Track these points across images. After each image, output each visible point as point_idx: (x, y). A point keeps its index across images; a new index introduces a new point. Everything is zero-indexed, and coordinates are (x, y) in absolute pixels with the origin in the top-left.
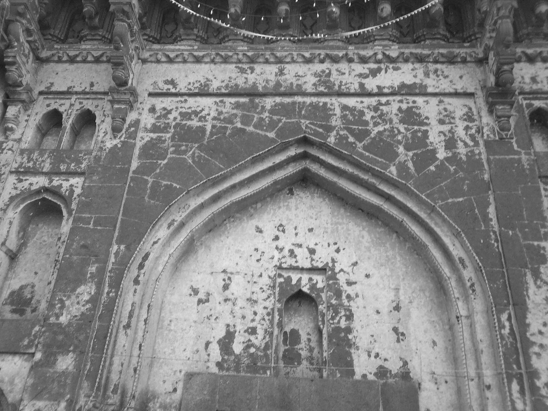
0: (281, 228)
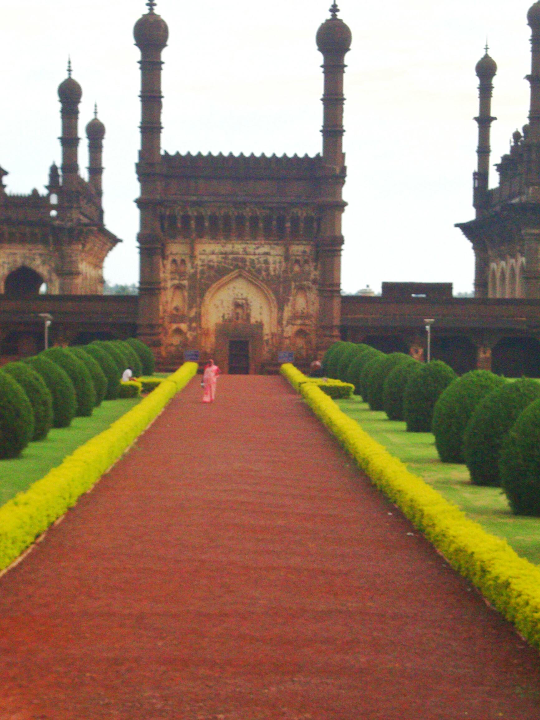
0: (234, 288)
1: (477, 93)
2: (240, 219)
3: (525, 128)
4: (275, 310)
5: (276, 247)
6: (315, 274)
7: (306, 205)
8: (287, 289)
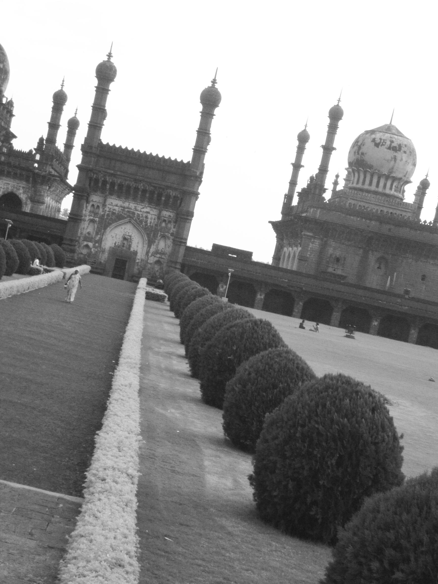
1: (296, 149)
2: (136, 189)
3: (316, 175)
4: (146, 246)
5: (155, 210)
6: (173, 230)
7: (176, 189)
8: (155, 236)
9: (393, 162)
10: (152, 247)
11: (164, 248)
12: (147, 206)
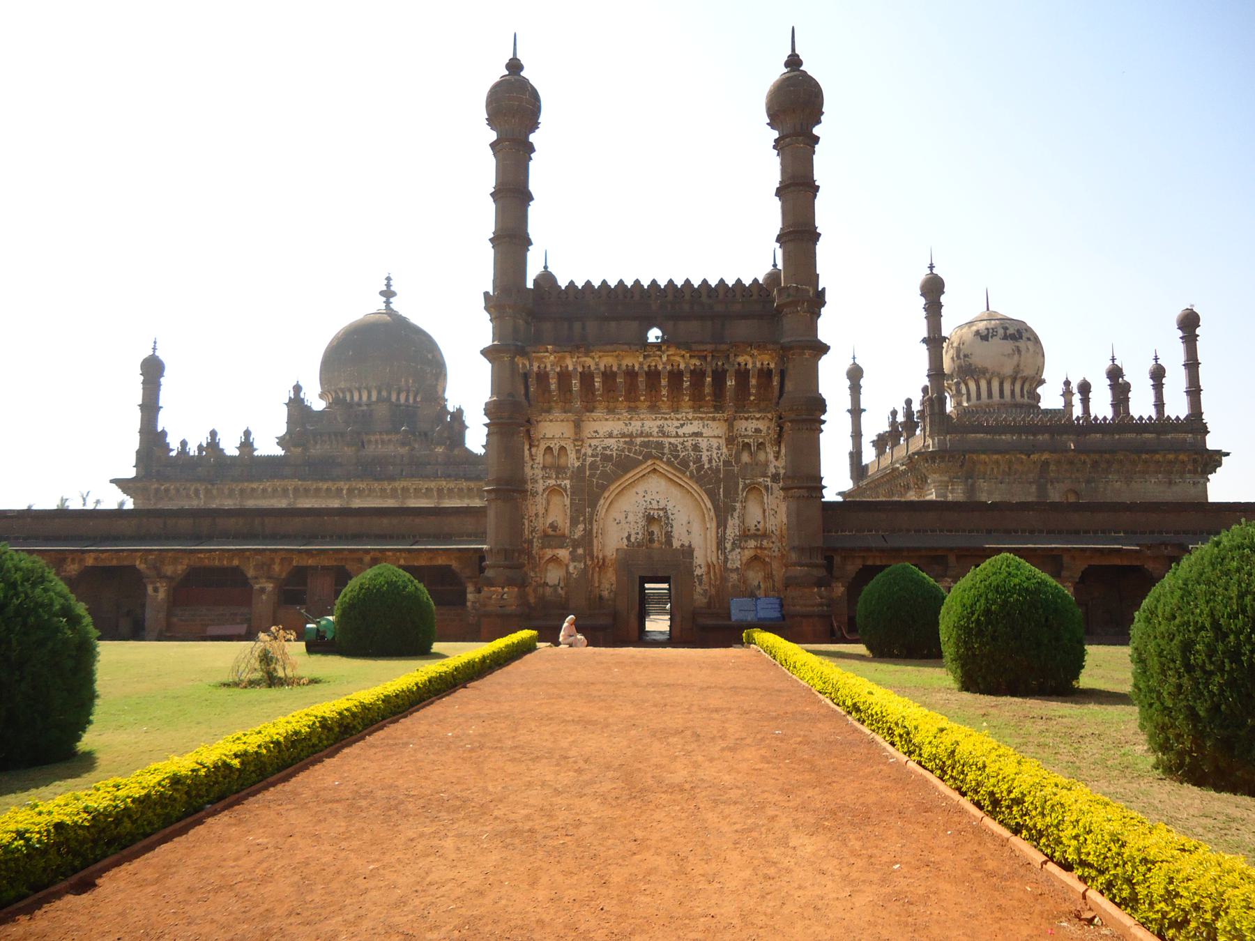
0: (646, 492)
2: (653, 375)
3: (909, 402)
4: (713, 525)
7: (761, 346)
8: (731, 493)
9: (1016, 357)
10: (730, 522)
11: (760, 518)
12: (690, 416)
